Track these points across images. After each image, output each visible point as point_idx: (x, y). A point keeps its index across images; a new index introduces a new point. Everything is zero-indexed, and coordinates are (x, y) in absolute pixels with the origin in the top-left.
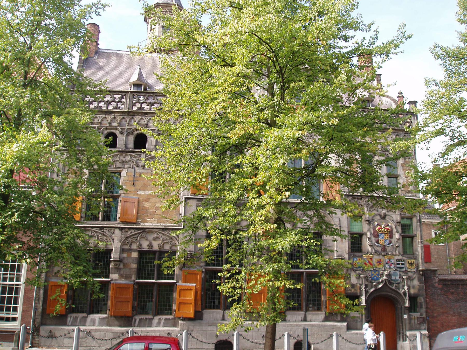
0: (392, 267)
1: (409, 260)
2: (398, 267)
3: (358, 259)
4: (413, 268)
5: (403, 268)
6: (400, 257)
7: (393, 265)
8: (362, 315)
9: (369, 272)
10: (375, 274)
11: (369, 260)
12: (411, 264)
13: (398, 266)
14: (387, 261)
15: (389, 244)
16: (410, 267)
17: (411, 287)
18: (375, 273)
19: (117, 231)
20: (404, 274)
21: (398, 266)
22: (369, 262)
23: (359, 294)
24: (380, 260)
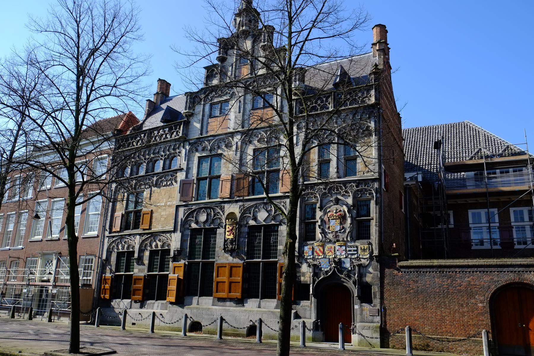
0: (343, 254)
4: (366, 254)
5: (354, 254)
8: (311, 304)
15: (340, 230)
19: (138, 237)
22: (320, 250)
23: (309, 283)
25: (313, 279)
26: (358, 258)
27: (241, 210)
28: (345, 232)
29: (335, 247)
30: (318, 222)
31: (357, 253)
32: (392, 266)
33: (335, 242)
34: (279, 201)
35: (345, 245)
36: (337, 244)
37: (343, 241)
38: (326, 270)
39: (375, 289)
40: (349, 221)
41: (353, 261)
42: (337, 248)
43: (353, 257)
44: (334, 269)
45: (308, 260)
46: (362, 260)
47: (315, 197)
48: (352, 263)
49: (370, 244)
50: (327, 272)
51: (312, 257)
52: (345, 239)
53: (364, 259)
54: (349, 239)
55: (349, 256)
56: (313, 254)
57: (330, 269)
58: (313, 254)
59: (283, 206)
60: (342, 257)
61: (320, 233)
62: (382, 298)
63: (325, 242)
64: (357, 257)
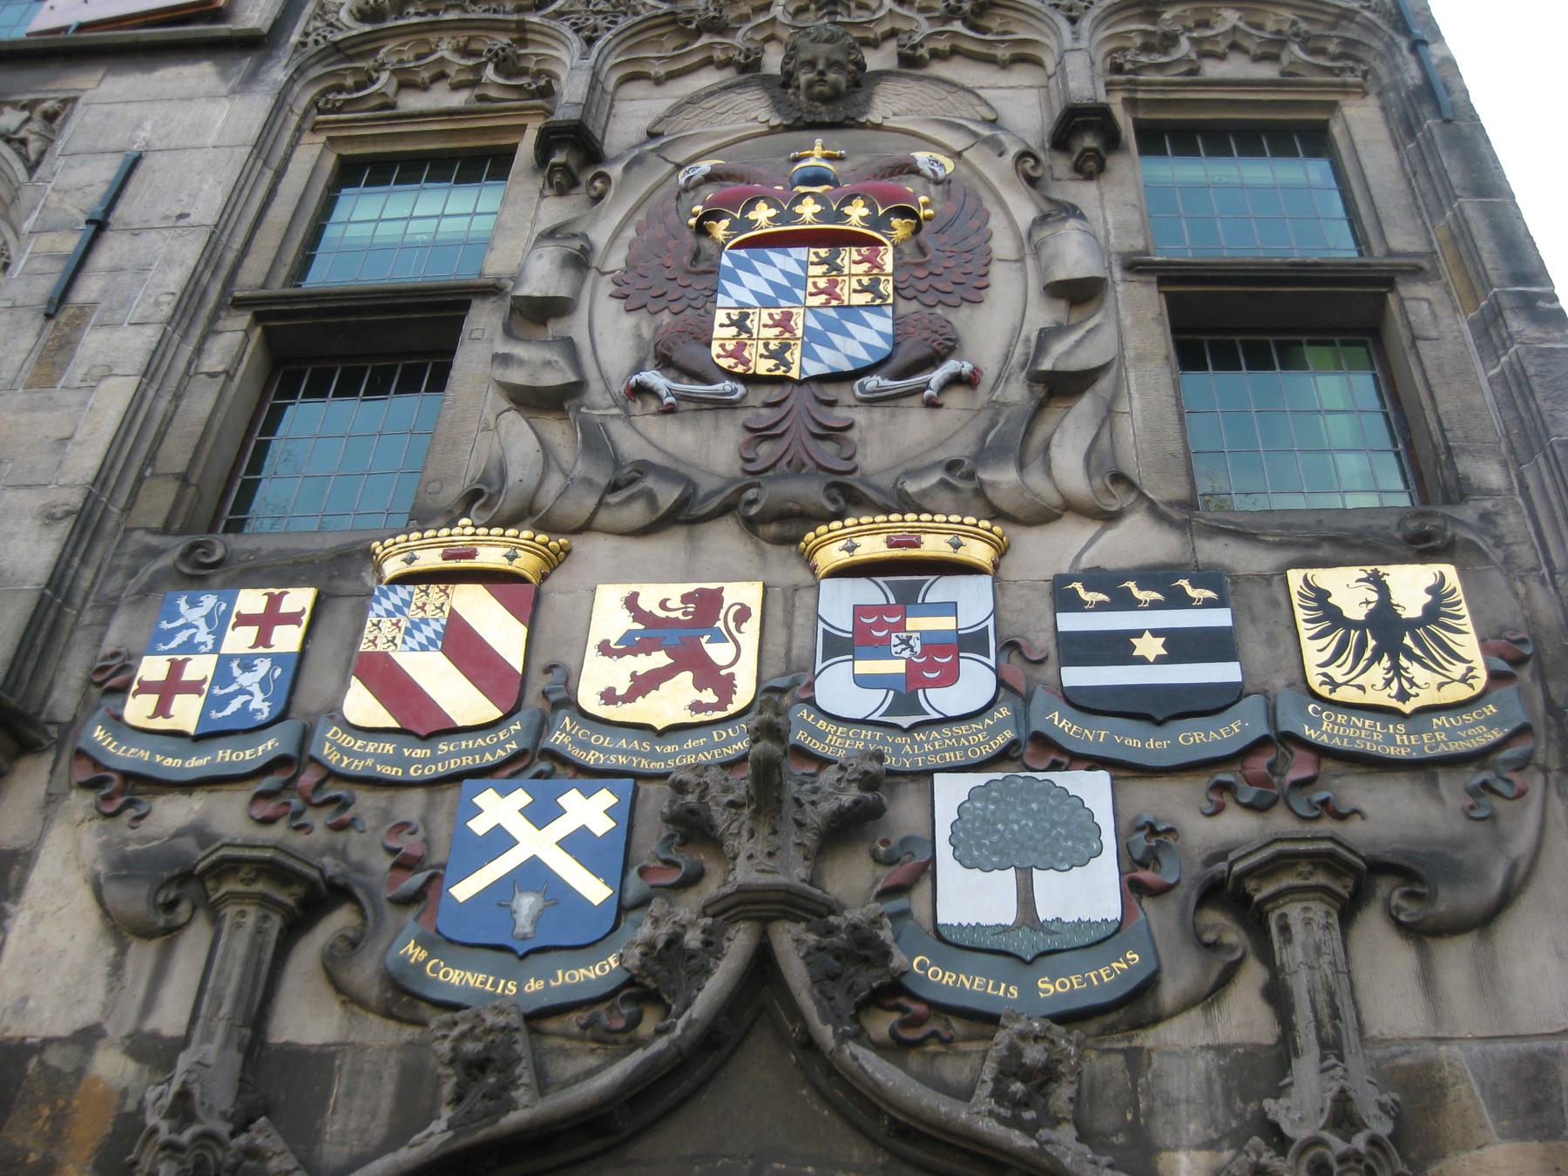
0: (943, 701)
1: (1348, 589)
2: (1085, 703)
3: (251, 600)
6: (1136, 541)
7: (975, 683)
9: (411, 806)
10: (539, 844)
12: (1386, 631)
13: (1075, 676)
14: (839, 604)
16: (1374, 684)
17: (1468, 1097)
18: (541, 814)
20: (1236, 825)
21: (1075, 676)
22: (462, 645)
24: (706, 606)
51: (268, 746)
53: (1423, 768)
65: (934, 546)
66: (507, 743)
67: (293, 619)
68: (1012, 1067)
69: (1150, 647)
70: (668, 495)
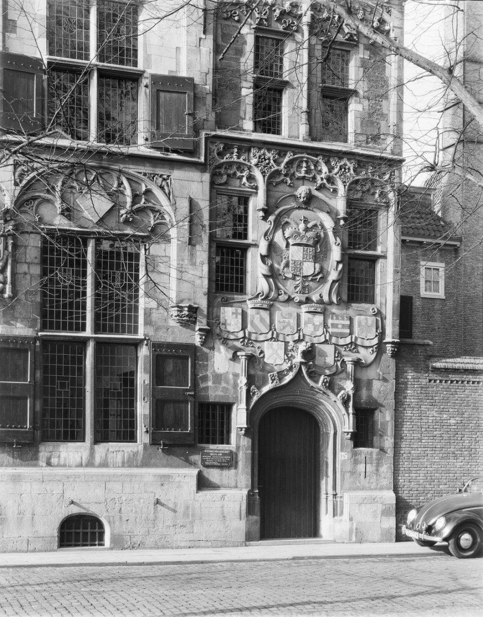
11: (262, 312)
15: (314, 275)
25: (248, 391)
26: (353, 346)
27: (21, 176)
28: (323, 280)
29: (298, 316)
30: (256, 246)
31: (351, 333)
32: (422, 366)
33: (301, 303)
34: (148, 169)
35: (324, 313)
36: (304, 308)
37: (321, 302)
38: (277, 369)
39: (385, 417)
40: (336, 253)
41: (342, 350)
42: (304, 317)
43: (342, 342)
44: (300, 369)
45: (230, 343)
46: (361, 350)
47: (251, 178)
48: (338, 355)
49: (379, 313)
50: (281, 375)
51: (241, 335)
52: (326, 298)
53: (367, 347)
54: (334, 299)
55: (334, 340)
56: (244, 328)
57: (291, 368)
58: (244, 328)
59: (162, 188)
60: (315, 340)
61: (266, 276)
62: (398, 436)
63: (275, 300)
64: (351, 343)
65: (319, 310)
66: (269, 336)
67: (239, 314)
68: (323, 382)
69: (340, 326)
70: (286, 297)
